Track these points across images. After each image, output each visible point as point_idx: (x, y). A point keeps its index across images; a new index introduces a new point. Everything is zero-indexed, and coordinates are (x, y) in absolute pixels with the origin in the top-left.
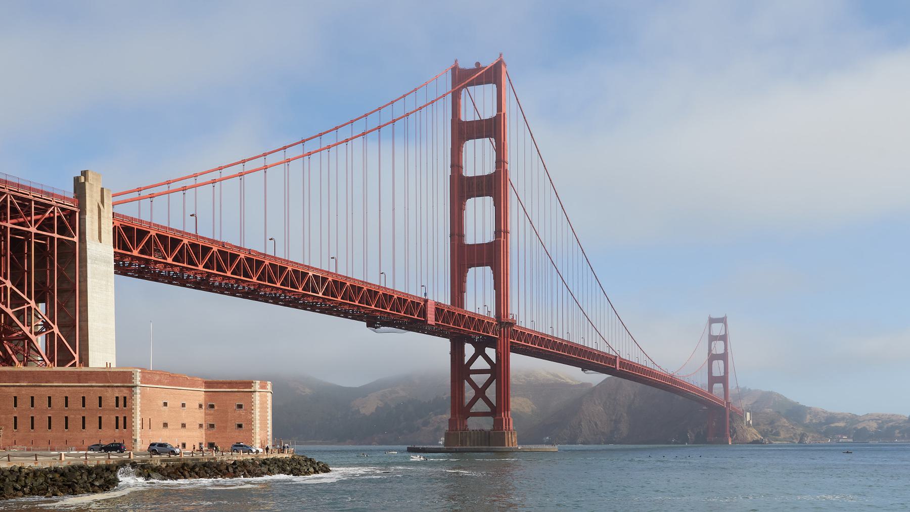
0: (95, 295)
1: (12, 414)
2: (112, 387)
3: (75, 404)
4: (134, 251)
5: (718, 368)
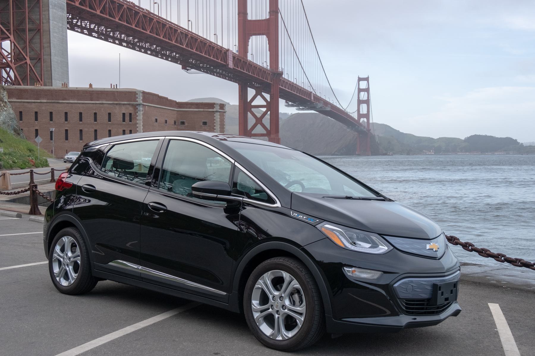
0: (55, 34)
1: (34, 126)
2: (120, 104)
4: (76, 2)
5: (364, 109)
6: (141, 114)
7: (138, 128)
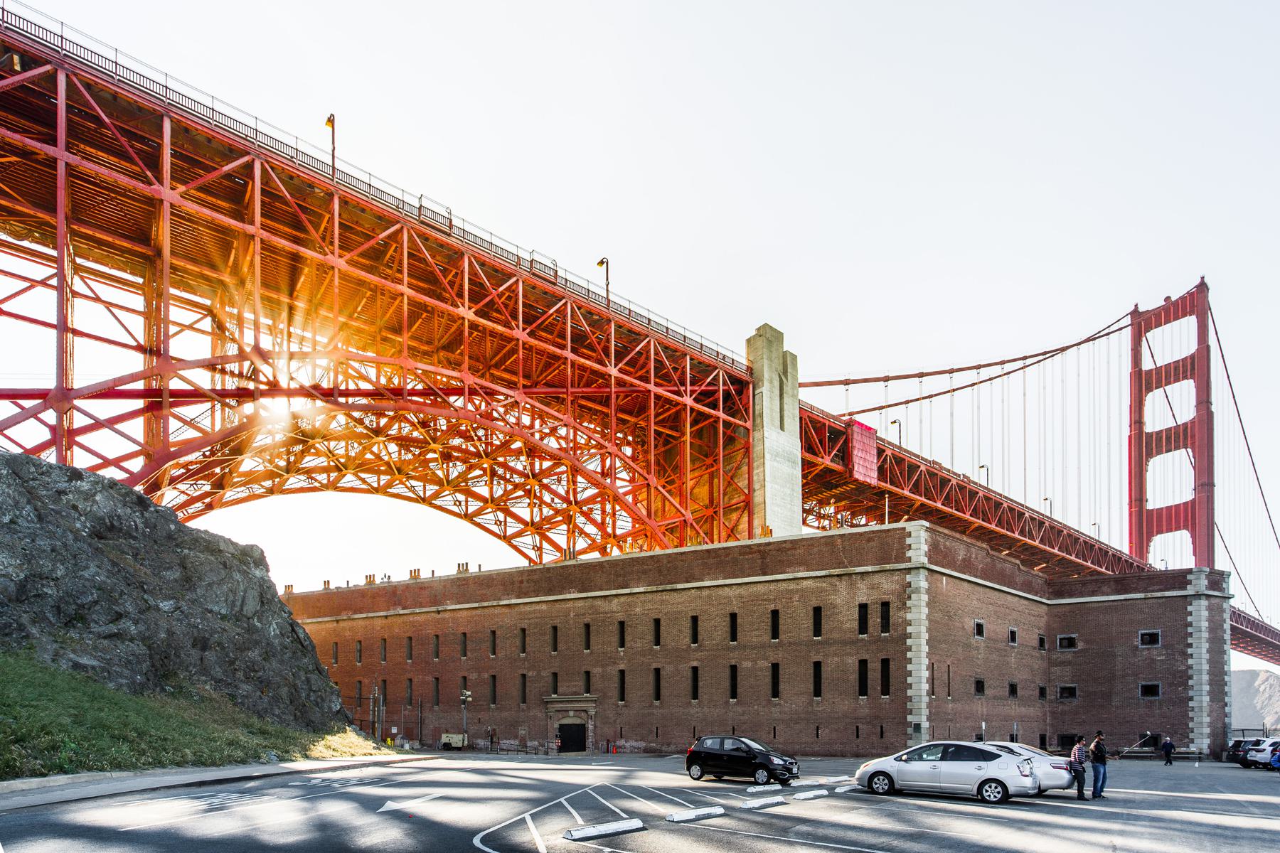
1: (615, 663)
3: (755, 632)
6: (923, 604)
7: (910, 650)
